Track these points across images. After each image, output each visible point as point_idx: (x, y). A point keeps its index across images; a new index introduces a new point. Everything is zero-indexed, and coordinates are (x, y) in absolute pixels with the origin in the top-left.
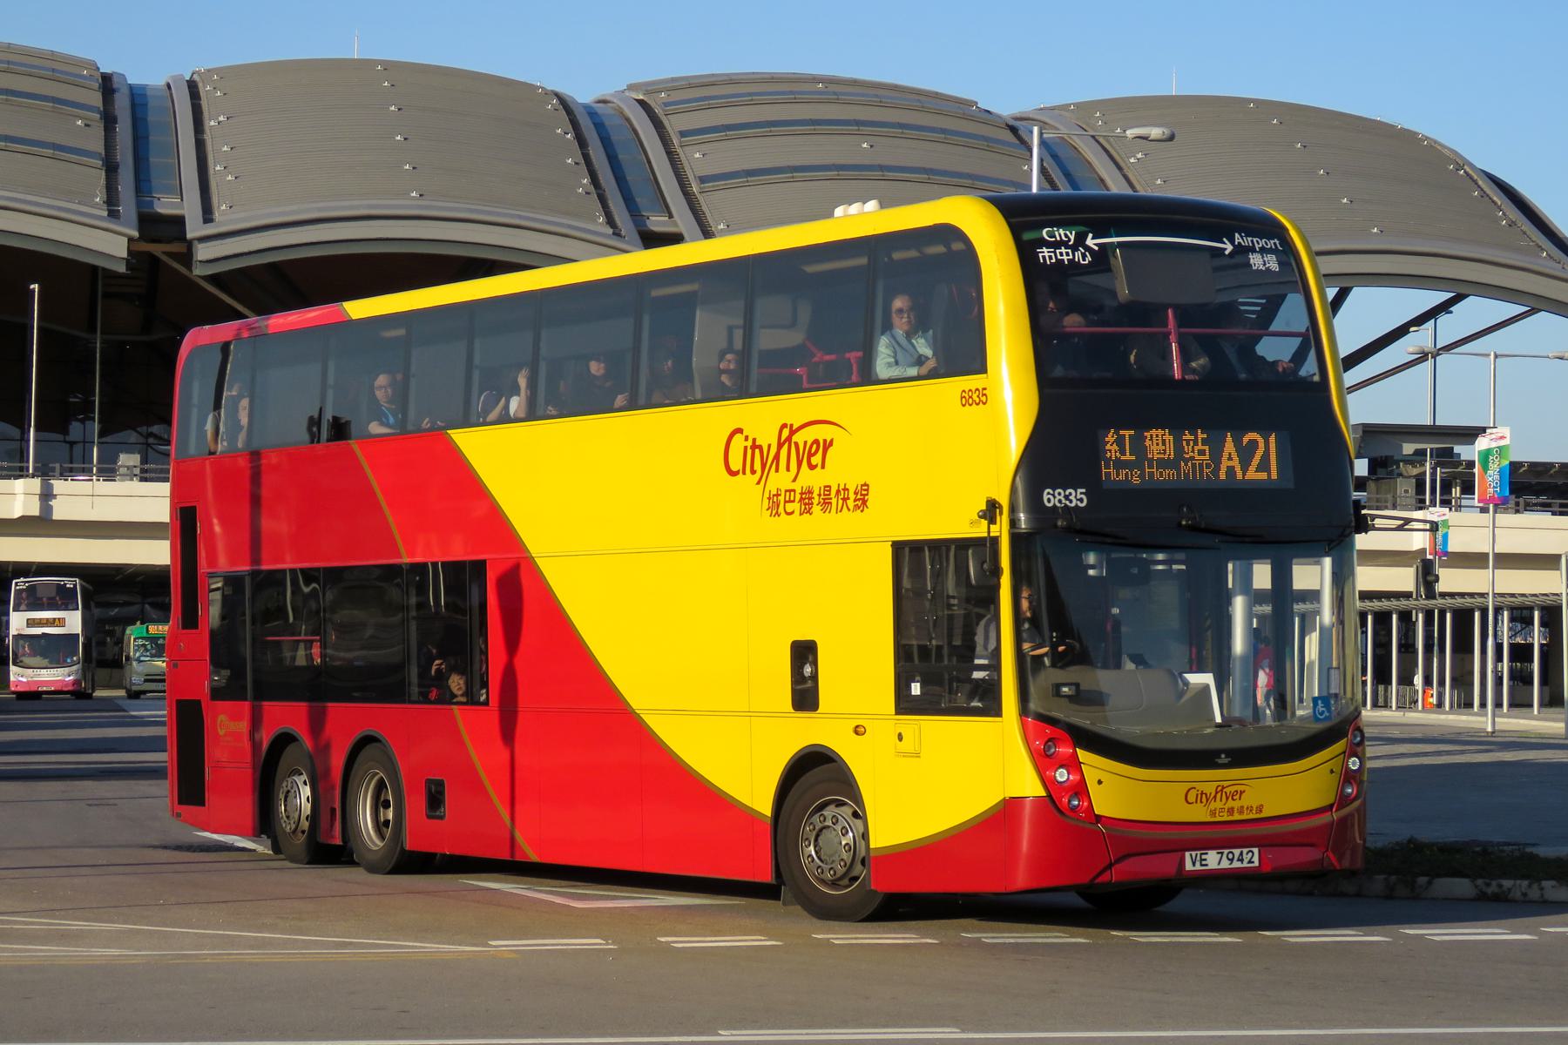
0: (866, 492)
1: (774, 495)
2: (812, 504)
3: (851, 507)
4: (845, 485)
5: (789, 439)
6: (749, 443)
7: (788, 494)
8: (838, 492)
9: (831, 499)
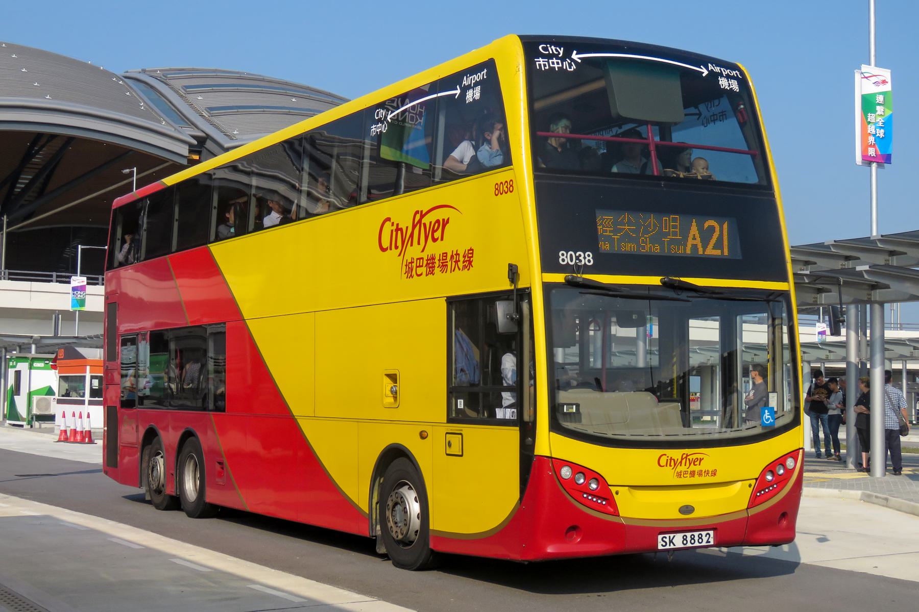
0: (470, 255)
1: (409, 263)
2: (434, 267)
3: (461, 267)
4: (457, 250)
5: (420, 221)
6: (394, 228)
7: (418, 261)
8: (452, 257)
9: (447, 262)
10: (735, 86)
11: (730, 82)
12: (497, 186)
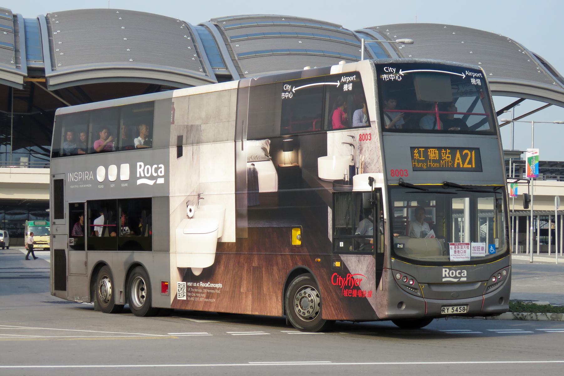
10: (479, 82)
11: (476, 80)
12: (360, 136)
